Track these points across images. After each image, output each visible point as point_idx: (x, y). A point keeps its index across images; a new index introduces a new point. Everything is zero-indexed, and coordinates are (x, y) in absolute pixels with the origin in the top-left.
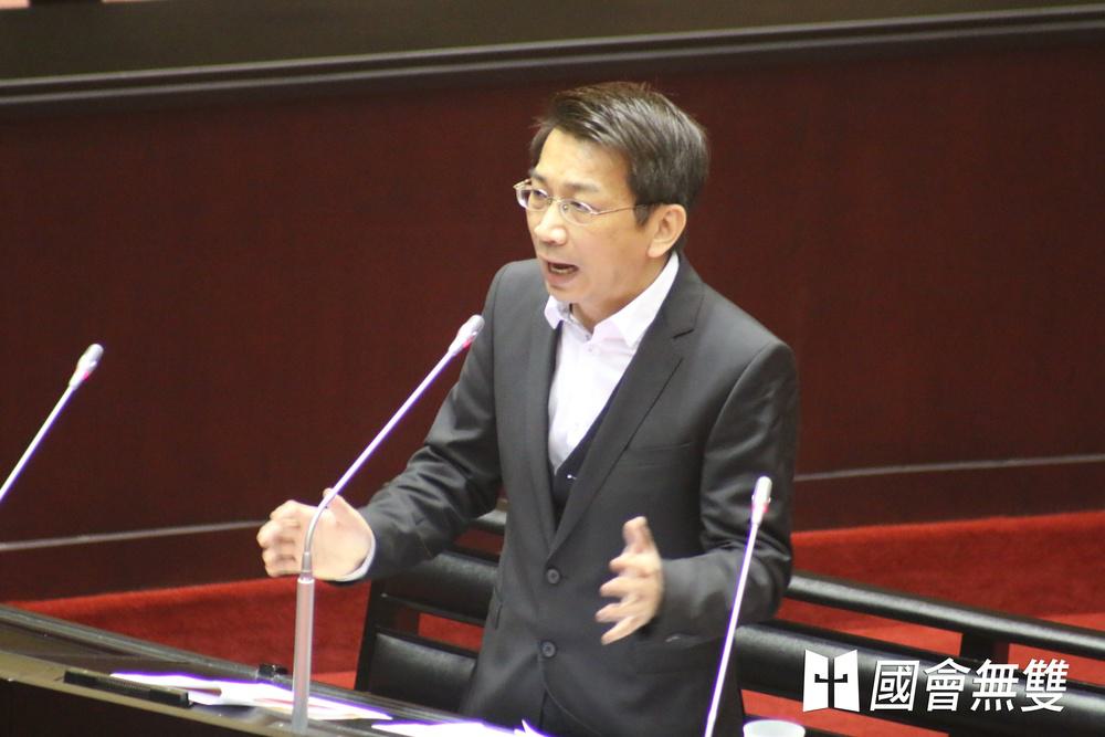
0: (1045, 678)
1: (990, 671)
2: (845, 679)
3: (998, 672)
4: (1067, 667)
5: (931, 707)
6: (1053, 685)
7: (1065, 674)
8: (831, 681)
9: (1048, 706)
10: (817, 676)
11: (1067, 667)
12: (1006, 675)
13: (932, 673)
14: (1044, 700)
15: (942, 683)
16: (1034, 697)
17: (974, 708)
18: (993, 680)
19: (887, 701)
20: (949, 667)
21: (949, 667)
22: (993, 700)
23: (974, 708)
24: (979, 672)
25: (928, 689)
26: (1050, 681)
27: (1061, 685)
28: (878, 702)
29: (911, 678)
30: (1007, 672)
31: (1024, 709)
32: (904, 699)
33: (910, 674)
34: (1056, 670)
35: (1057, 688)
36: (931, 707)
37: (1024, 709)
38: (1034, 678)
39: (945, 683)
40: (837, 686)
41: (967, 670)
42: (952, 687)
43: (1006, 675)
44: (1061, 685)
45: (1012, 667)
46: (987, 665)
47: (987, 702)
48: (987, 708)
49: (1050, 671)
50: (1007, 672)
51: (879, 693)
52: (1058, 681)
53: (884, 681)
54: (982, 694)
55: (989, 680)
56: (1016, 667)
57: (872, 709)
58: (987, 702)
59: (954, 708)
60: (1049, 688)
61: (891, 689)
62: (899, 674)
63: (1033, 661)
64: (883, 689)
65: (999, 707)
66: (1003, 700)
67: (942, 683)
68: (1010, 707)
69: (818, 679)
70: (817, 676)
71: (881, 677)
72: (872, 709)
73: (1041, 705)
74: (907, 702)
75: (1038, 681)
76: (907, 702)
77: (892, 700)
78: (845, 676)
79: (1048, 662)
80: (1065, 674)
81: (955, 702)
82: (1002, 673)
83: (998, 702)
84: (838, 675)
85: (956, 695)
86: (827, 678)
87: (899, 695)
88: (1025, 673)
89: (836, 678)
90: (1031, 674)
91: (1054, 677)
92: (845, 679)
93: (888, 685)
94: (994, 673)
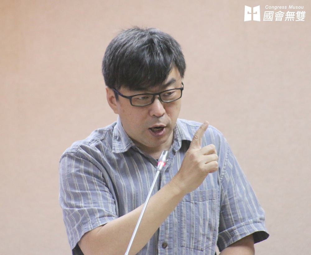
0: (301, 15)
1: (289, 13)
2: (256, 13)
3: (291, 13)
5: (276, 20)
6: (302, 16)
8: (252, 13)
9: (301, 20)
13: (277, 14)
15: (278, 16)
16: (298, 18)
17: (286, 20)
18: (289, 15)
20: (280, 12)
22: (289, 19)
23: (286, 20)
24: (286, 14)
25: (276, 17)
26: (302, 15)
28: (265, 19)
29: (272, 15)
30: (292, 13)
31: (296, 21)
32: (270, 19)
33: (271, 14)
35: (303, 17)
36: (276, 20)
37: (296, 21)
40: (254, 15)
41: (284, 13)
42: (281, 16)
43: (292, 14)
45: (294, 13)
46: (288, 12)
47: (288, 19)
48: (288, 20)
51: (265, 17)
52: (304, 15)
53: (266, 15)
54: (287, 18)
58: (288, 19)
59: (281, 20)
60: (302, 17)
61: (268, 17)
62: (269, 14)
63: (298, 11)
64: (266, 17)
65: (291, 20)
66: (292, 19)
67: (278, 16)
68: (293, 20)
69: (248, 13)
73: (300, 20)
74: (271, 19)
75: (299, 15)
76: (271, 19)
79: (301, 12)
81: (281, 19)
82: (292, 14)
84: (254, 12)
89: (254, 12)
92: (256, 13)
93: (267, 16)
94: (290, 14)
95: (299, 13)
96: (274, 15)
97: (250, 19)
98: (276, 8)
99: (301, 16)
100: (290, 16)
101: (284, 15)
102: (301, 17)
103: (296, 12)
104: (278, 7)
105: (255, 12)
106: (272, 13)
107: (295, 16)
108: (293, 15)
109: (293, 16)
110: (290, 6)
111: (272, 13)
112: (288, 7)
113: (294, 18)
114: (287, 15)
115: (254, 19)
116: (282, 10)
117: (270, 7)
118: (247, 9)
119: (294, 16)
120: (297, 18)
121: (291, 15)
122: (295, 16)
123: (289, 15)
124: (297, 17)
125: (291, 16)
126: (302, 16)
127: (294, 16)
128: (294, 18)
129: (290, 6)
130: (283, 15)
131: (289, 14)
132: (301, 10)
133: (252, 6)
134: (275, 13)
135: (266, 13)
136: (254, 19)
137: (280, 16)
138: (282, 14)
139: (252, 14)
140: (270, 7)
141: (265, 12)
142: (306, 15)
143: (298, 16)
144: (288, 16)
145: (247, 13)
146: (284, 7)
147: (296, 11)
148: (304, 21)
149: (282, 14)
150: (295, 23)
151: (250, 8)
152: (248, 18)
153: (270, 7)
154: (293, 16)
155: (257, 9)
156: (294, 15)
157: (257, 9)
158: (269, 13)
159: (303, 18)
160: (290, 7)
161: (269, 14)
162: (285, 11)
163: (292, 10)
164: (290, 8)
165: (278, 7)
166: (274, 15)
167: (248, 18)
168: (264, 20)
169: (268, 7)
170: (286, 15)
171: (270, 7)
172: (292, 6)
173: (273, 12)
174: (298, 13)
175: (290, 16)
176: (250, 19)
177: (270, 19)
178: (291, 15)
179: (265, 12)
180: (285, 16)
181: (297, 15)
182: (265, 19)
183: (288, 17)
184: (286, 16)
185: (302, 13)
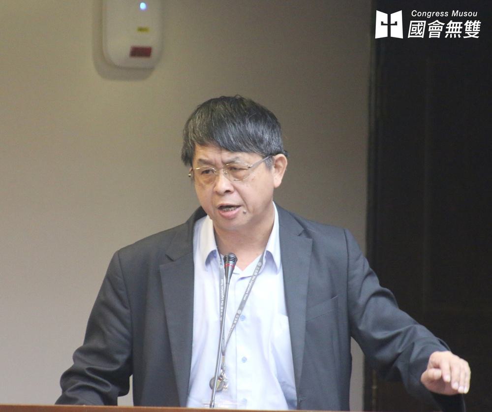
0: (472, 27)
1: (452, 25)
2: (396, 24)
3: (455, 25)
4: (480, 23)
5: (430, 37)
6: (475, 29)
7: (479, 28)
8: (389, 25)
9: (473, 36)
10: (382, 23)
11: (480, 23)
12: (458, 26)
13: (432, 25)
14: (472, 34)
15: (434, 28)
16: (468, 33)
17: (446, 37)
18: (453, 28)
19: (414, 35)
20: (437, 23)
21: (437, 23)
22: (453, 34)
23: (446, 37)
24: (448, 25)
26: (474, 28)
27: (478, 29)
28: (411, 35)
29: (423, 27)
30: (458, 25)
31: (464, 37)
32: (420, 34)
33: (422, 25)
34: (476, 24)
35: (477, 30)
36: (430, 37)
37: (464, 37)
38: (468, 27)
39: (435, 28)
40: (391, 26)
41: (443, 24)
42: (438, 30)
43: (458, 26)
44: (478, 29)
46: (451, 22)
47: (451, 35)
48: (451, 37)
49: (474, 24)
50: (458, 25)
51: (411, 32)
52: (477, 28)
53: (413, 28)
54: (449, 32)
55: (451, 28)
56: (462, 23)
57: (409, 37)
58: (451, 35)
59: (439, 37)
60: (474, 30)
61: (416, 30)
62: (419, 25)
63: (468, 21)
64: (413, 30)
65: (455, 36)
66: (457, 34)
67: (434, 28)
68: (459, 36)
69: (382, 24)
70: (382, 23)
71: (412, 27)
72: (409, 37)
73: (471, 36)
74: (422, 35)
75: (470, 28)
76: (422, 35)
77: (416, 34)
78: (396, 23)
80: (479, 28)
81: (439, 35)
83: (455, 35)
84: (392, 22)
85: (439, 33)
86: (391, 26)
87: (419, 33)
88: (465, 25)
90: (467, 25)
91: (476, 27)
92: (396, 24)
93: (414, 29)
94: (453, 25)
95: (468, 24)
96: (427, 27)
97: (386, 35)
98: (430, 15)
99: (472, 29)
100: (454, 29)
101: (444, 27)
102: (472, 31)
103: (464, 22)
104: (433, 13)
105: (394, 23)
106: (423, 23)
107: (463, 30)
108: (460, 27)
109: (459, 30)
110: (453, 11)
111: (423, 23)
112: (450, 14)
113: (461, 32)
114: (449, 28)
115: (392, 36)
116: (441, 19)
117: (420, 14)
118: (381, 16)
119: (461, 30)
120: (466, 33)
121: (456, 28)
122: (463, 30)
123: (453, 28)
124: (466, 30)
125: (456, 30)
126: (475, 29)
127: (461, 30)
128: (461, 32)
129: (453, 11)
130: (442, 27)
131: (452, 26)
132: (473, 19)
133: (389, 12)
134: (429, 24)
135: (413, 23)
136: (392, 36)
137: (437, 28)
138: (440, 25)
139: (389, 25)
140: (419, 14)
141: (411, 22)
142: (481, 27)
143: (468, 30)
144: (451, 29)
145: (381, 23)
146: (444, 14)
147: (464, 20)
148: (477, 37)
149: (440, 25)
150: (461, 42)
151: (387, 15)
152: (381, 32)
153: (420, 14)
154: (459, 30)
155: (397, 17)
156: (462, 28)
157: (397, 17)
158: (417, 23)
159: (477, 33)
160: (455, 13)
161: (419, 25)
162: (445, 20)
163: (456, 19)
164: (455, 15)
165: (433, 13)
166: (427, 27)
167: (381, 32)
168: (409, 36)
169: (417, 13)
170: (447, 28)
171: (419, 14)
172: (457, 11)
173: (425, 22)
174: (468, 24)
175: (454, 29)
176: (386, 35)
177: (420, 34)
178: (456, 28)
179: (411, 22)
180: (445, 30)
181: (466, 28)
182: (411, 35)
183: (451, 31)
184: (447, 30)
185: (474, 24)
